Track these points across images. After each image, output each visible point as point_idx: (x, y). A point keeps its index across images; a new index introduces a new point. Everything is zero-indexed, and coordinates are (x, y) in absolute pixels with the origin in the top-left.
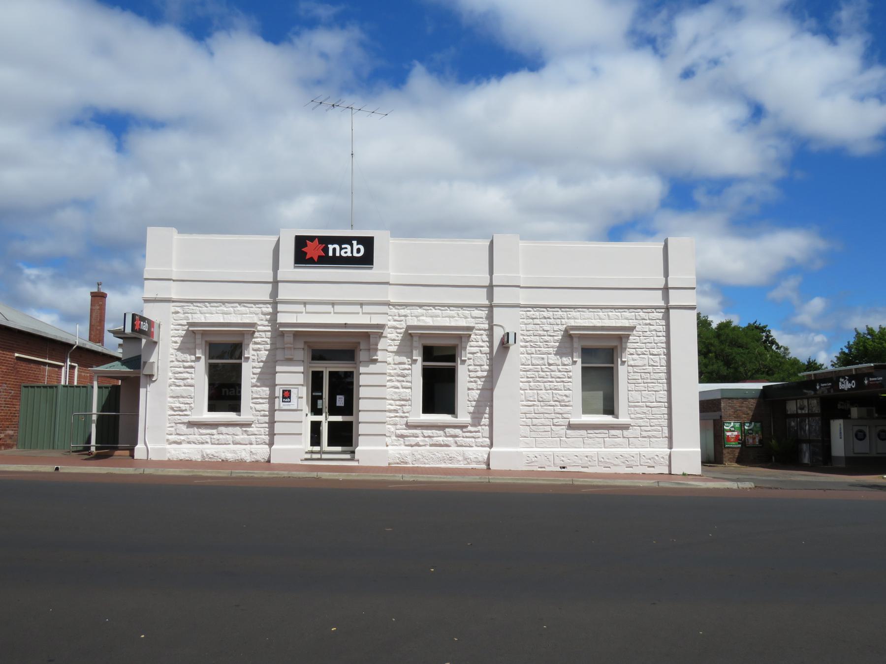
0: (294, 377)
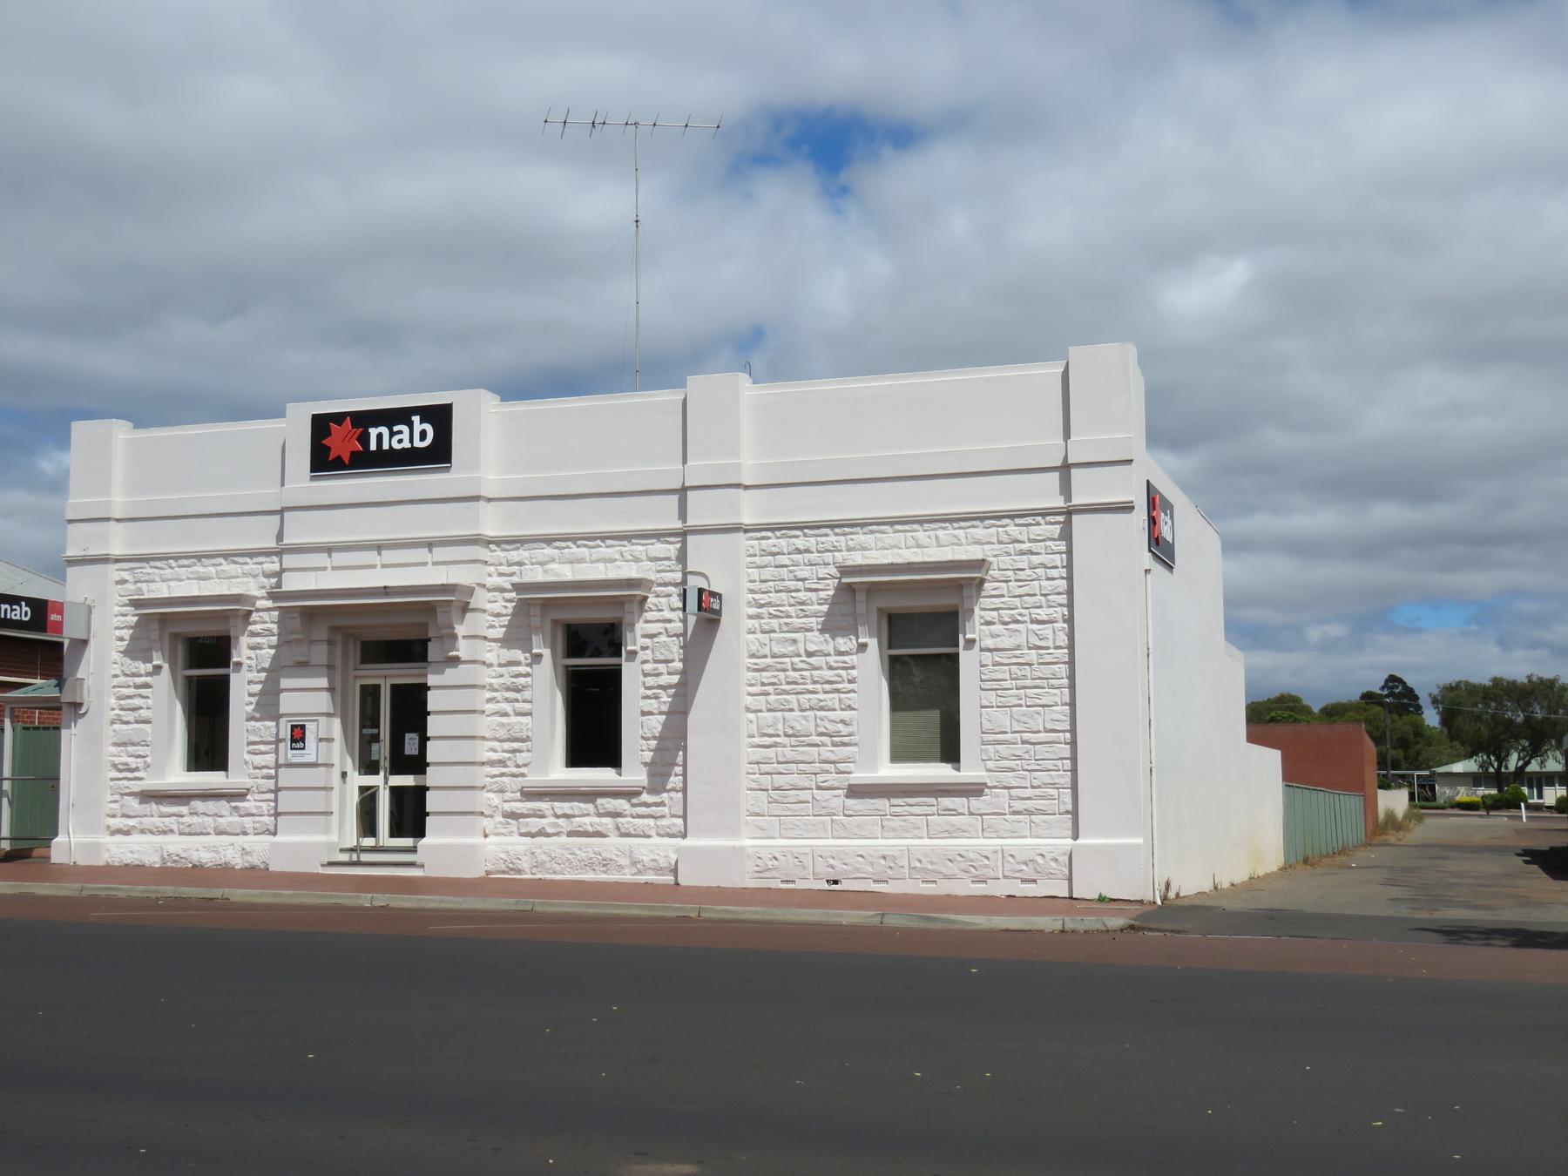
0: (309, 697)
